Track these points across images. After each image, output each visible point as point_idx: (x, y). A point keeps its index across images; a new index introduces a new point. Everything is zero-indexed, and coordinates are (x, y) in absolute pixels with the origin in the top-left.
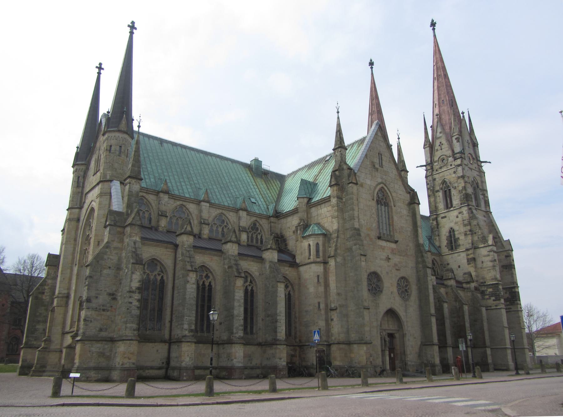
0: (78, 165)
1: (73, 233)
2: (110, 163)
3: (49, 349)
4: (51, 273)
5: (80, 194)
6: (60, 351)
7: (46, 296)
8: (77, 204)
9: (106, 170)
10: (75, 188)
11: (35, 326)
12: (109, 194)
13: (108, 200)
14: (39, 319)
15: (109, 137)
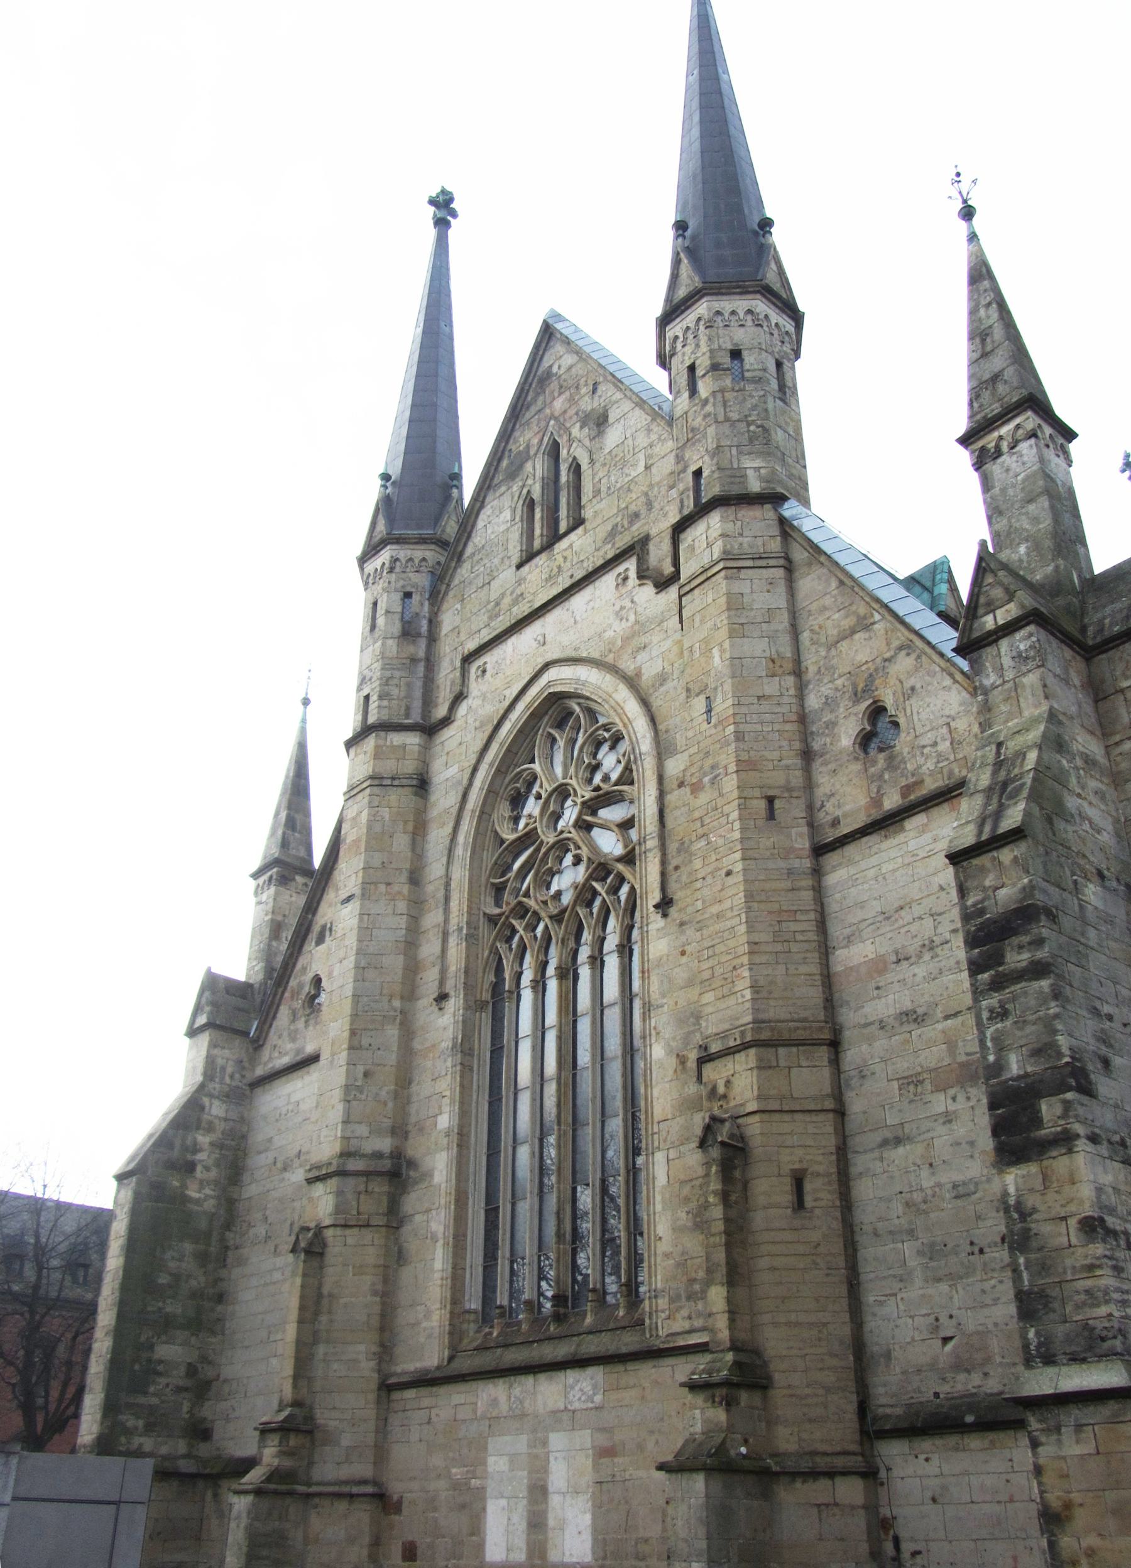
0: (399, 541)
1: (401, 842)
2: (749, 425)
3: (309, 1484)
4: (223, 1069)
5: (421, 668)
6: (373, 1495)
7: (202, 1184)
8: (408, 708)
9: (734, 451)
10: (390, 642)
11: (151, 1347)
12: (782, 562)
13: (781, 588)
14: (169, 1309)
15: (718, 313)
